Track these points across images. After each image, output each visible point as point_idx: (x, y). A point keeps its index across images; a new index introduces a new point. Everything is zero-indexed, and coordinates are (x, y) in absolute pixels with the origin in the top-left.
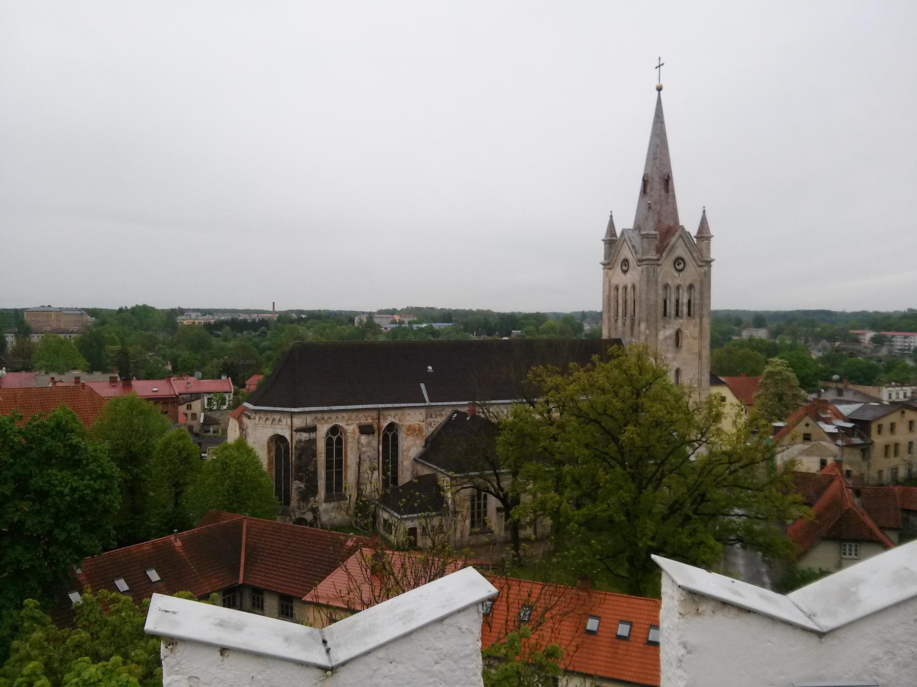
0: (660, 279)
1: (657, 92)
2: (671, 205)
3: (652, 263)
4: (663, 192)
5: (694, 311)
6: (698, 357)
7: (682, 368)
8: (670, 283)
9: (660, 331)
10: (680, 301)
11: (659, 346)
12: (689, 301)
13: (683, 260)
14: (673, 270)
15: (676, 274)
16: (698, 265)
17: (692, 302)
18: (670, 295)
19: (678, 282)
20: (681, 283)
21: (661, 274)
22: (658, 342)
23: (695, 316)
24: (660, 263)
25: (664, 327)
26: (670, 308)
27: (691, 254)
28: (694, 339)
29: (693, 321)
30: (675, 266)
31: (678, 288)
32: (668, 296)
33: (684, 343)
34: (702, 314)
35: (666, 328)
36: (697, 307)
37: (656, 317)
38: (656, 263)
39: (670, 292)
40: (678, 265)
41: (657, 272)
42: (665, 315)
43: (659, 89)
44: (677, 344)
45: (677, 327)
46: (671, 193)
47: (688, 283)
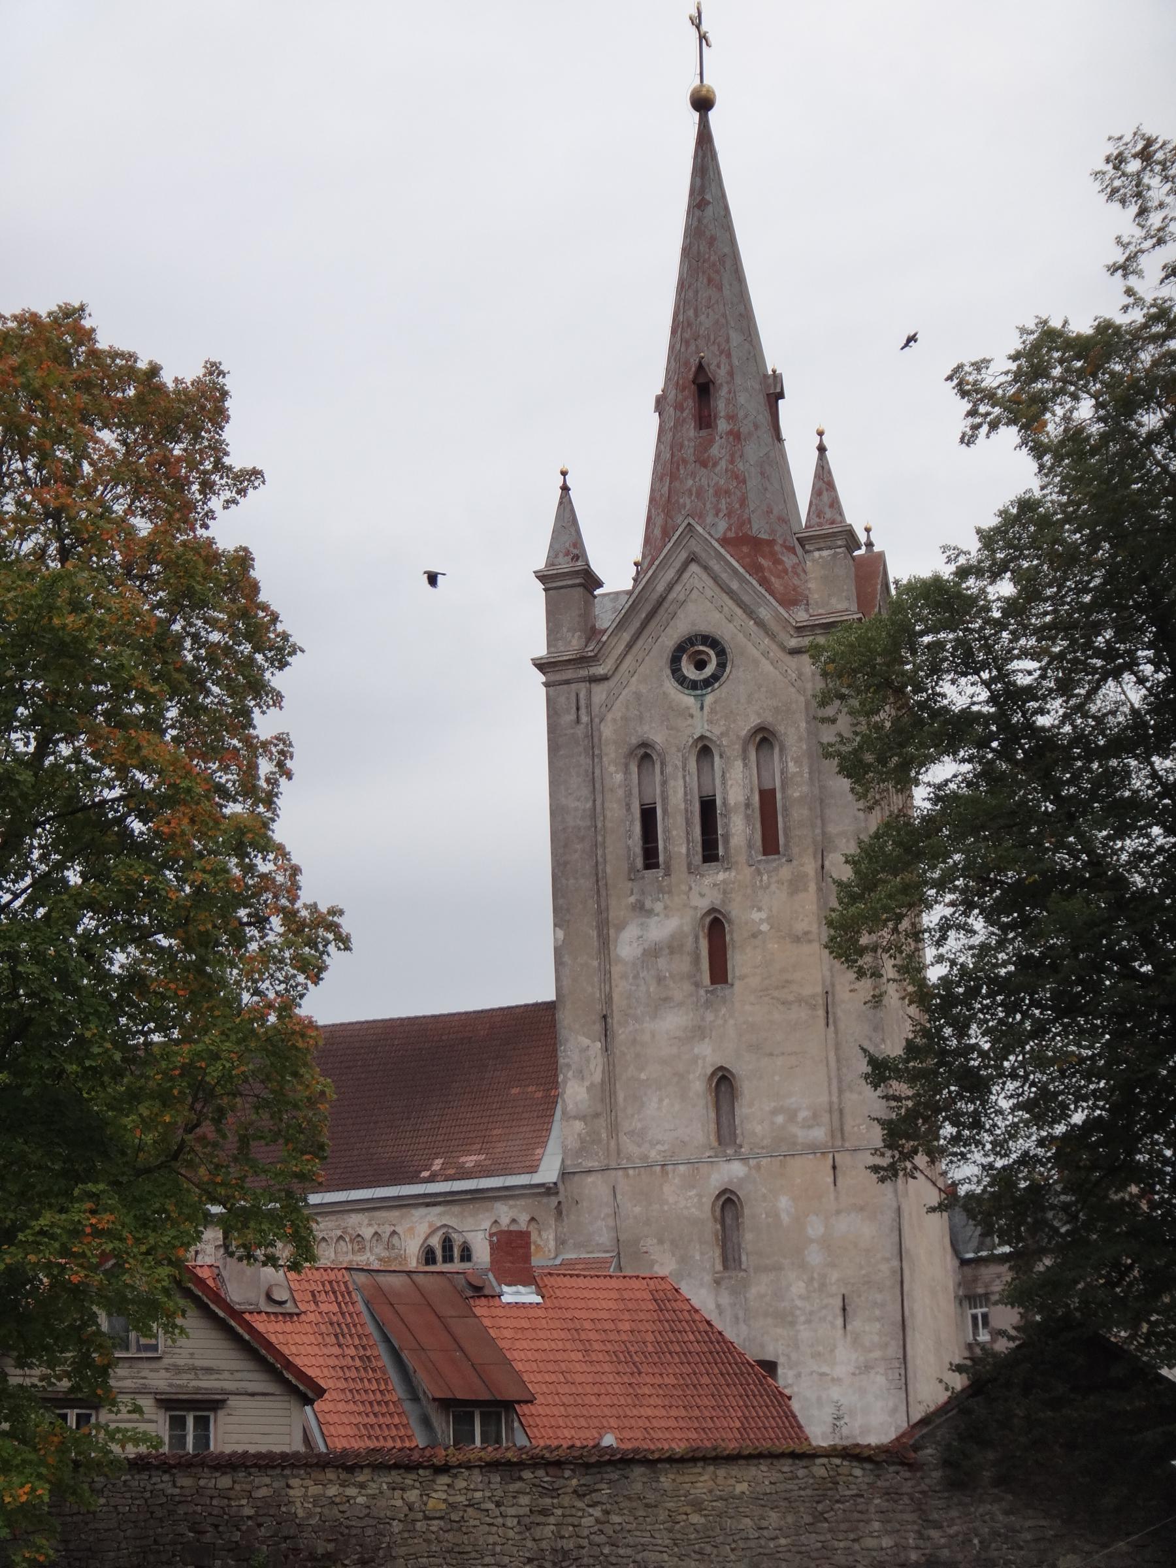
0: (607, 731)
1: (696, 115)
2: (723, 464)
3: (569, 674)
4: (690, 431)
5: (786, 829)
6: (821, 1013)
7: (740, 1069)
8: (658, 737)
9: (621, 927)
10: (719, 802)
11: (620, 988)
12: (767, 798)
13: (713, 642)
14: (670, 686)
15: (688, 700)
16: (783, 647)
17: (779, 796)
18: (664, 783)
19: (700, 727)
20: (717, 731)
21: (617, 712)
22: (616, 970)
23: (795, 850)
24: (600, 670)
25: (640, 909)
26: (667, 831)
27: (750, 613)
28: (797, 940)
29: (786, 872)
30: (676, 671)
31: (705, 750)
32: (658, 791)
33: (740, 961)
34: (824, 833)
35: (650, 913)
36: (799, 813)
37: (598, 878)
38: (583, 673)
39: (662, 773)
40: (700, 665)
41: (589, 706)
42: (650, 858)
43: (702, 103)
44: (719, 973)
45: (704, 904)
46: (722, 425)
47: (745, 726)
